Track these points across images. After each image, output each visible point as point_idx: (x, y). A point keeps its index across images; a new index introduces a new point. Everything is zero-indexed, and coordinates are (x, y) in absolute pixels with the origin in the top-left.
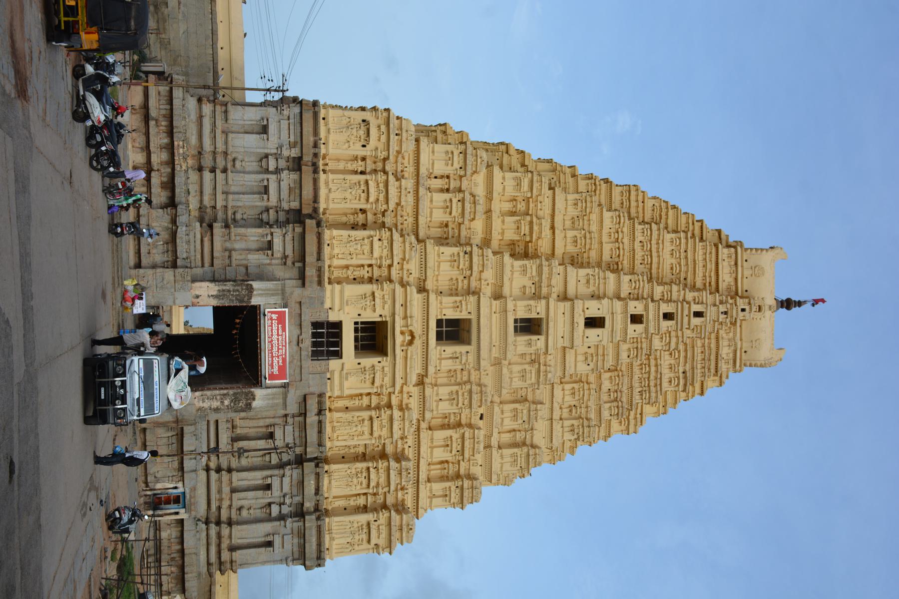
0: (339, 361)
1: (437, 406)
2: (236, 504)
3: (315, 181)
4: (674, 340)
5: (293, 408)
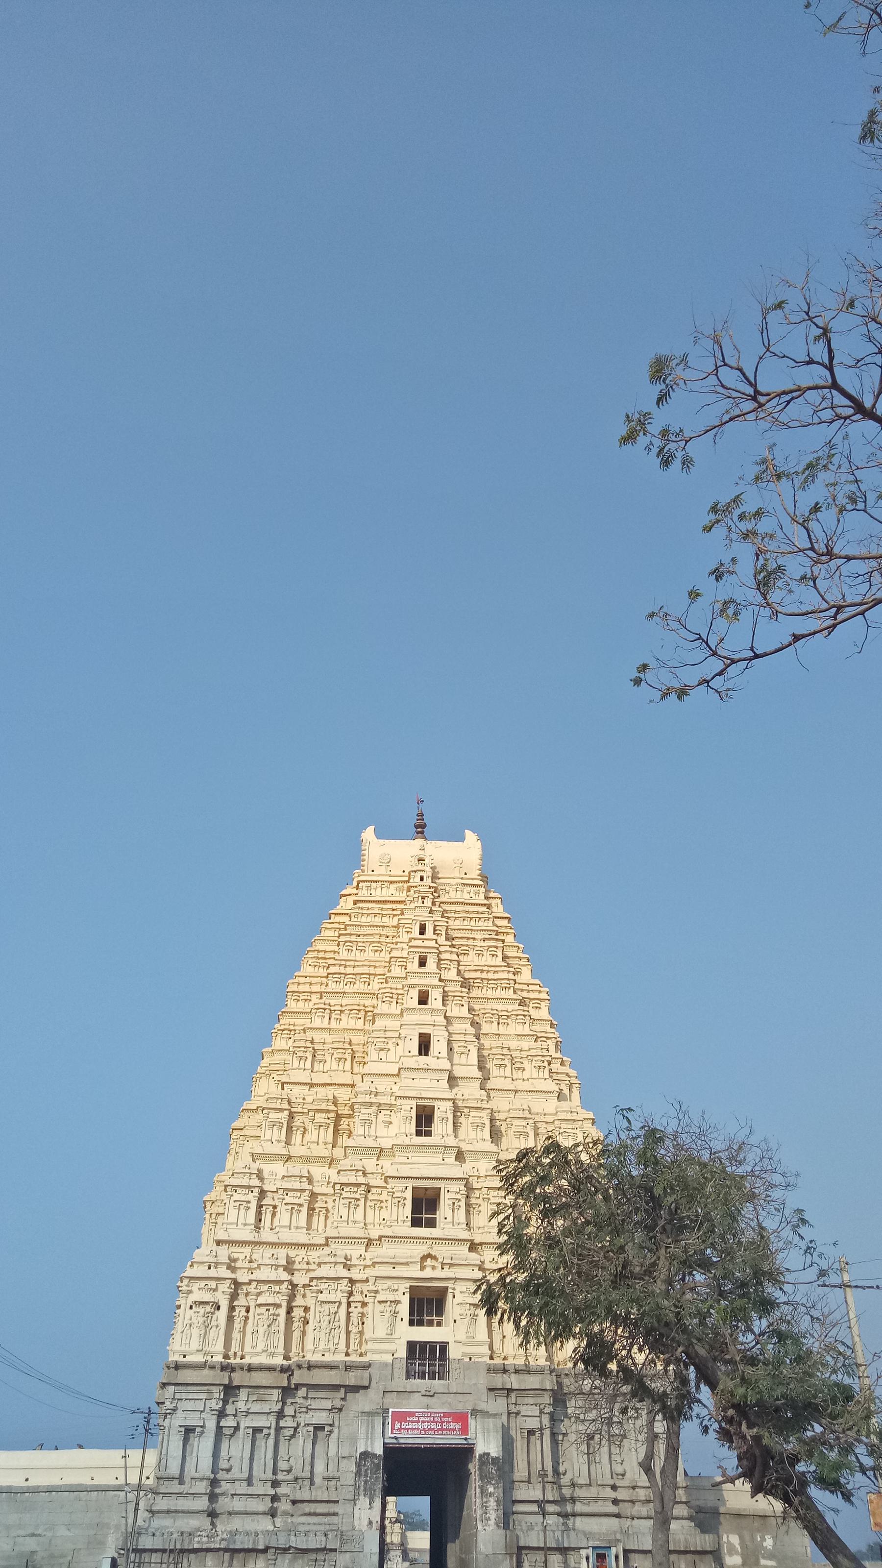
3: (250, 1368)
5: (499, 1405)
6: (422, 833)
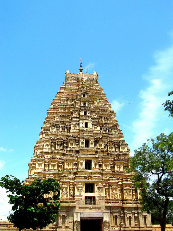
0: (96, 197)
1: (108, 170)
2: (134, 226)
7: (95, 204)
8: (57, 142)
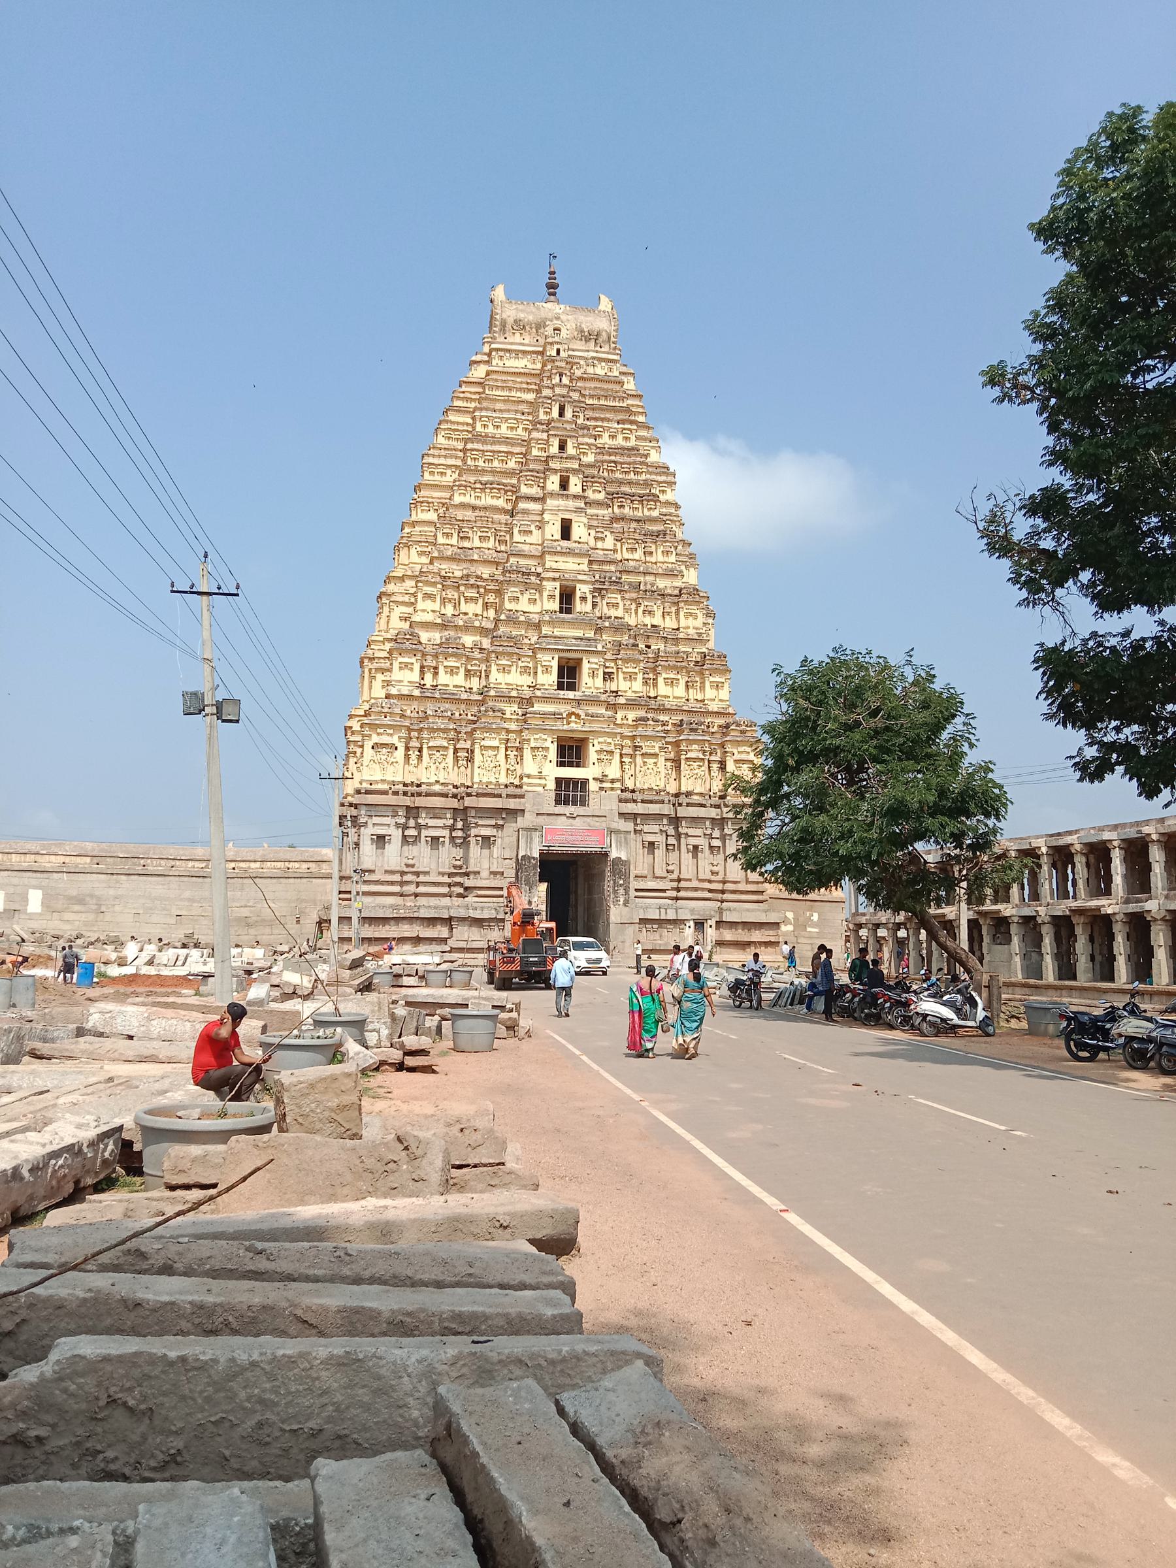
0: (591, 780)
4: (586, 440)
5: (630, 826)
6: (554, 294)
7: (583, 803)
8: (462, 588)
